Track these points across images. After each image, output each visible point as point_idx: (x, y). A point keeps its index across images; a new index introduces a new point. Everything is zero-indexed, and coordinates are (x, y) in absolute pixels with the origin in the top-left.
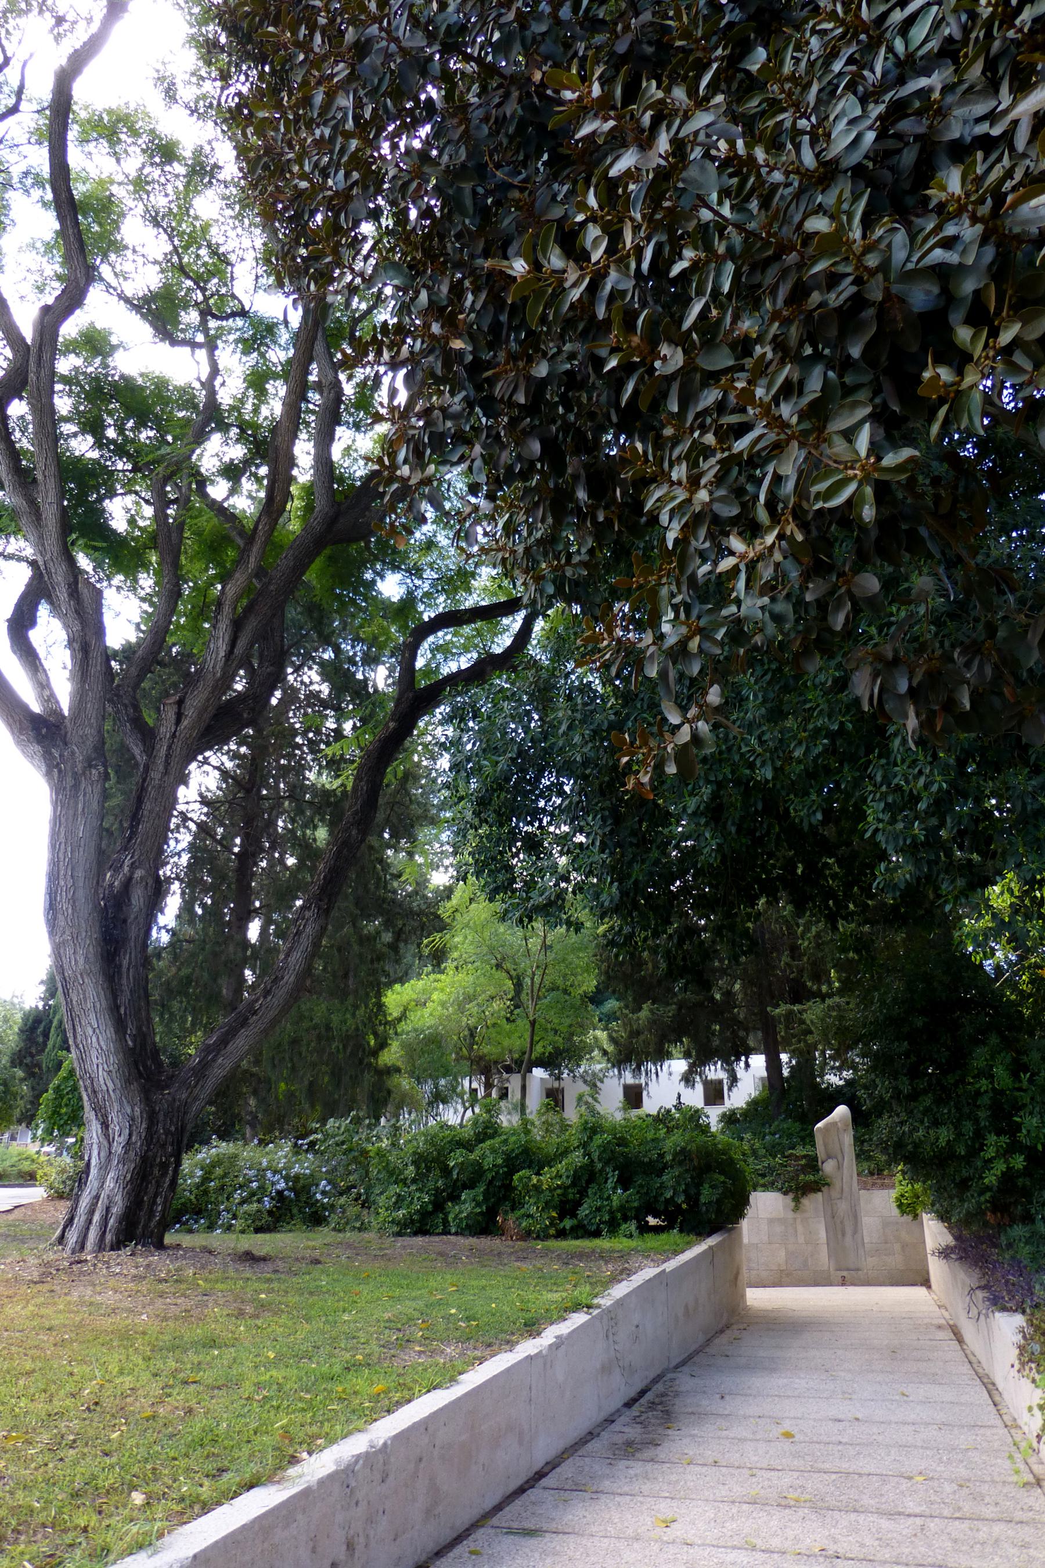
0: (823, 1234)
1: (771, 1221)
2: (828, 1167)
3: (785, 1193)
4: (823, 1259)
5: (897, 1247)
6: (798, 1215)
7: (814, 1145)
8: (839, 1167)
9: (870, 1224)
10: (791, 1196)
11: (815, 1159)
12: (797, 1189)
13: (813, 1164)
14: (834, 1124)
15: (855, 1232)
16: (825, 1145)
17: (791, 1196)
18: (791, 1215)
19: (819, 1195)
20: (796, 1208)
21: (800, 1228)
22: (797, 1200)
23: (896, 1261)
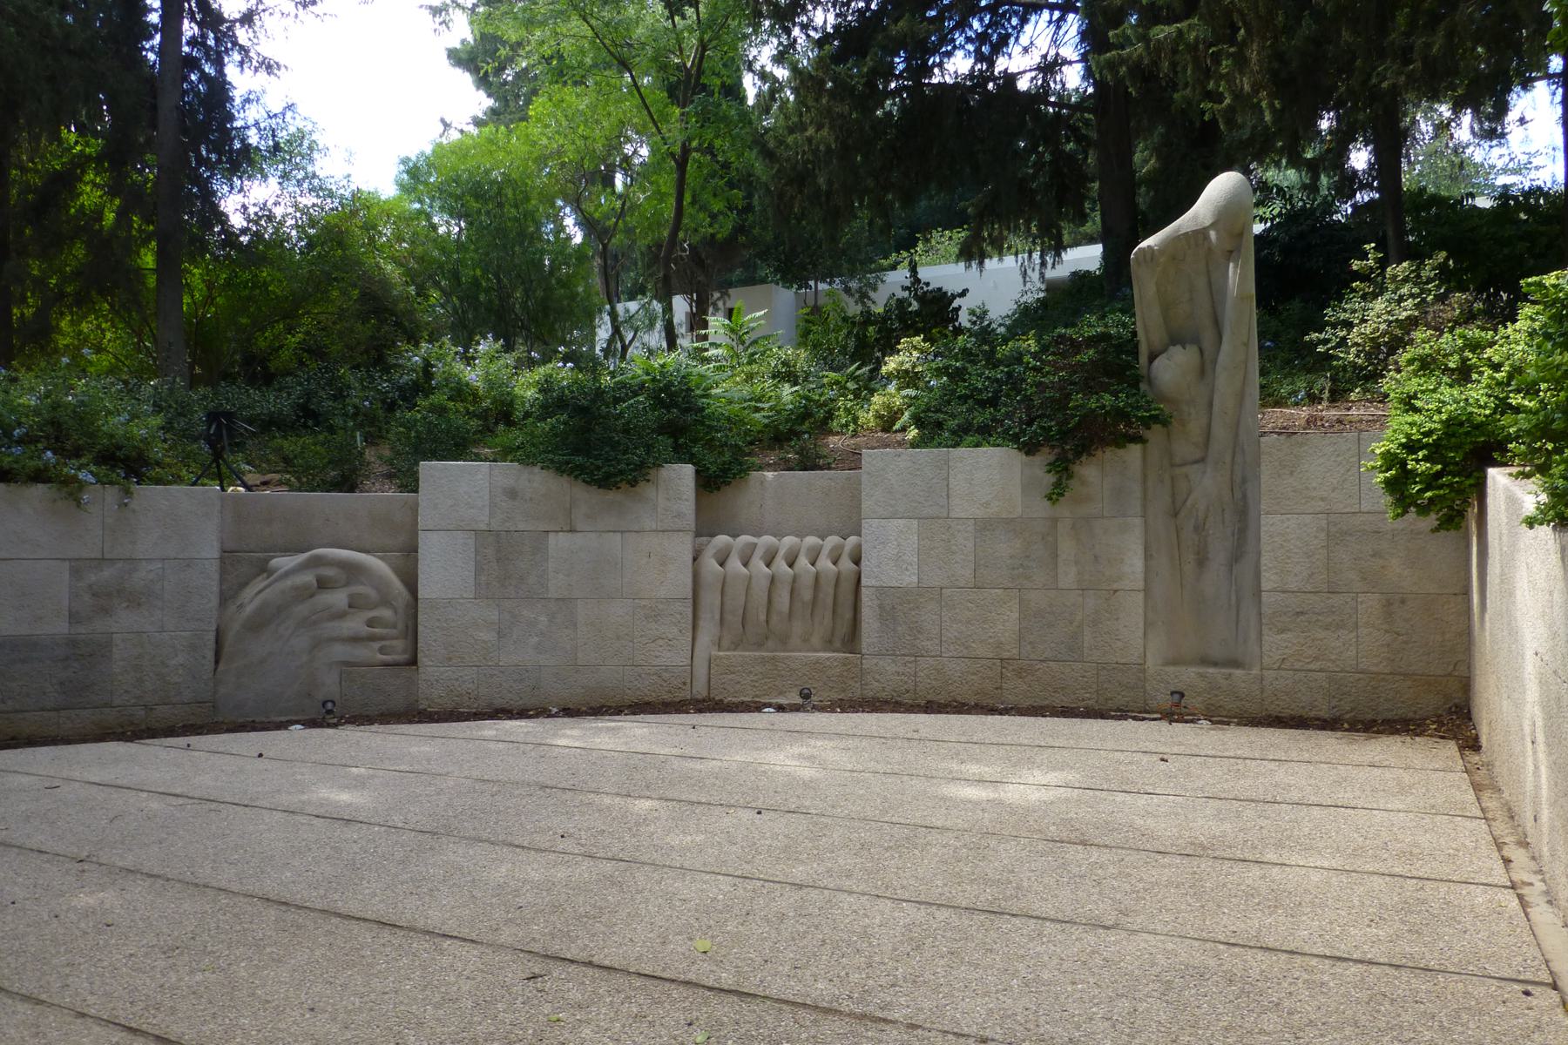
0: (1134, 564)
1: (984, 526)
2: (1171, 370)
3: (1029, 449)
4: (1132, 637)
5: (1370, 604)
6: (1064, 510)
7: (1129, 310)
8: (1205, 370)
9: (1286, 538)
10: (1044, 457)
11: (1129, 345)
12: (1065, 435)
13: (1120, 363)
14: (1200, 234)
15: (1236, 556)
16: (1166, 308)
17: (1044, 457)
18: (1042, 508)
19: (1135, 450)
20: (1056, 494)
21: (1067, 547)
22: (1062, 469)
23: (1358, 648)
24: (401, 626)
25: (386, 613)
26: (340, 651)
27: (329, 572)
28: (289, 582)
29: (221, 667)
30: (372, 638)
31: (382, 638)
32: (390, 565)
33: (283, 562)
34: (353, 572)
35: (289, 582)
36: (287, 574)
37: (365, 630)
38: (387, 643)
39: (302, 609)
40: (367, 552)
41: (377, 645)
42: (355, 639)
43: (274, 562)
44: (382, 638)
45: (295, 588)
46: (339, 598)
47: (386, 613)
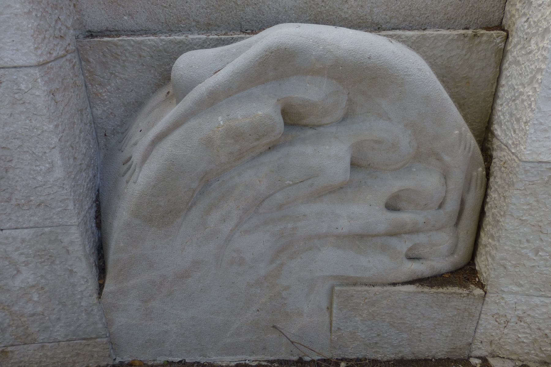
24: (452, 206)
25: (428, 181)
26: (332, 261)
27: (309, 92)
28: (218, 121)
29: (110, 286)
30: (395, 233)
31: (415, 231)
32: (433, 66)
33: (208, 65)
34: (362, 80)
35: (218, 121)
36: (213, 100)
37: (383, 220)
38: (422, 238)
39: (254, 178)
40: (376, 28)
41: (403, 245)
42: (360, 239)
43: (187, 63)
44: (415, 231)
45: (235, 134)
46: (329, 155)
47: (428, 181)
